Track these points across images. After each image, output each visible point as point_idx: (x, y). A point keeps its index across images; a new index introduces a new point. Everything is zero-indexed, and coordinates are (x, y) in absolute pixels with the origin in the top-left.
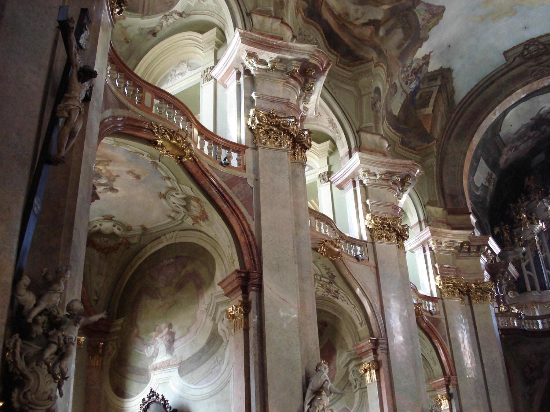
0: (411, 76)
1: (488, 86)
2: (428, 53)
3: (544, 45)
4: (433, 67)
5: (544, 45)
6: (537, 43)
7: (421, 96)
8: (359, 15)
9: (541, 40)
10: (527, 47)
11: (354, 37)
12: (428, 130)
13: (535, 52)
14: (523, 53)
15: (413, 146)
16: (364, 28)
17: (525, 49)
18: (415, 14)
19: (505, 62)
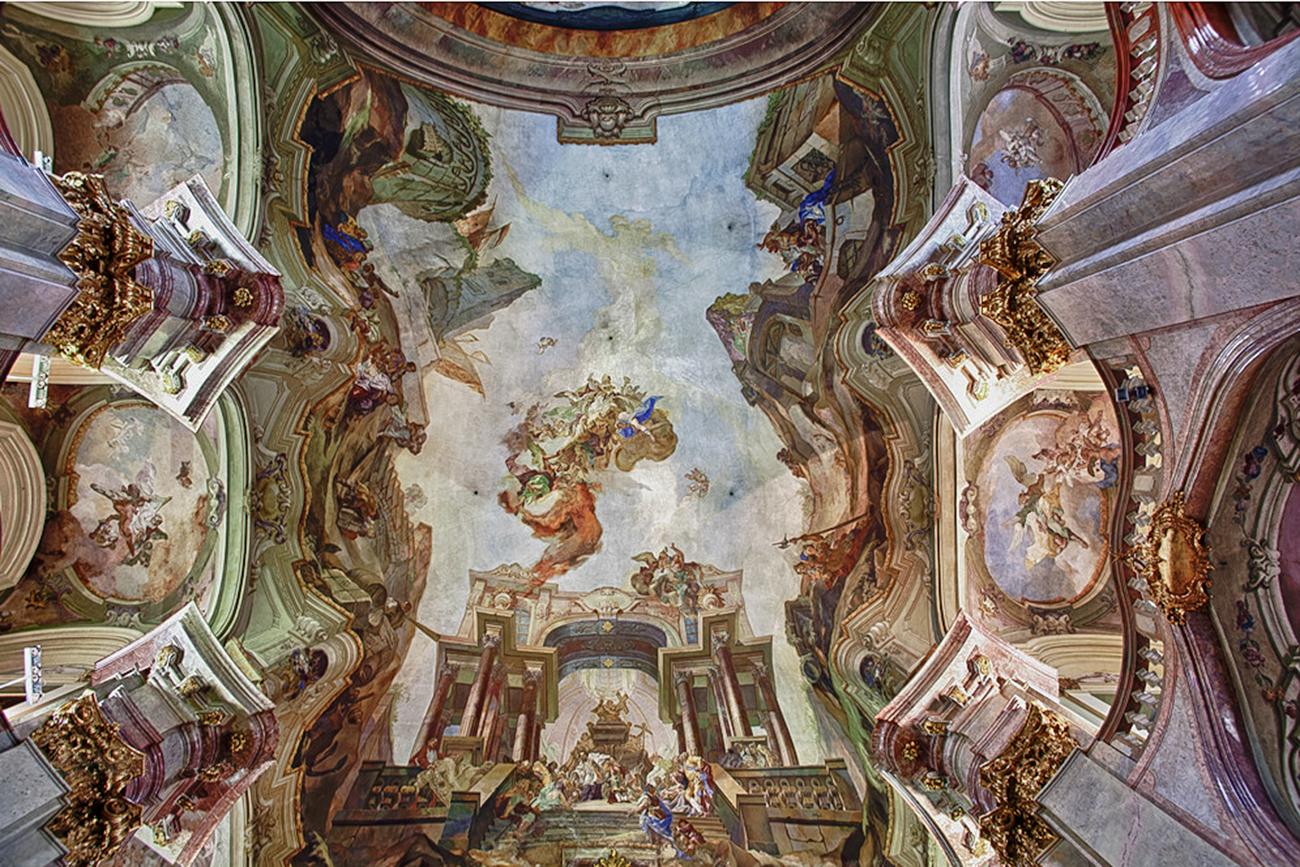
0: (810, 237)
1: (704, 86)
2: (766, 249)
3: (589, 120)
4: (769, 213)
5: (589, 120)
6: (599, 130)
7: (815, 180)
8: (822, 440)
9: (588, 133)
10: (616, 130)
11: (847, 428)
12: (837, 109)
13: (606, 109)
14: (626, 120)
15: (879, 110)
16: (828, 423)
17: (621, 128)
18: (751, 353)
19: (659, 118)
